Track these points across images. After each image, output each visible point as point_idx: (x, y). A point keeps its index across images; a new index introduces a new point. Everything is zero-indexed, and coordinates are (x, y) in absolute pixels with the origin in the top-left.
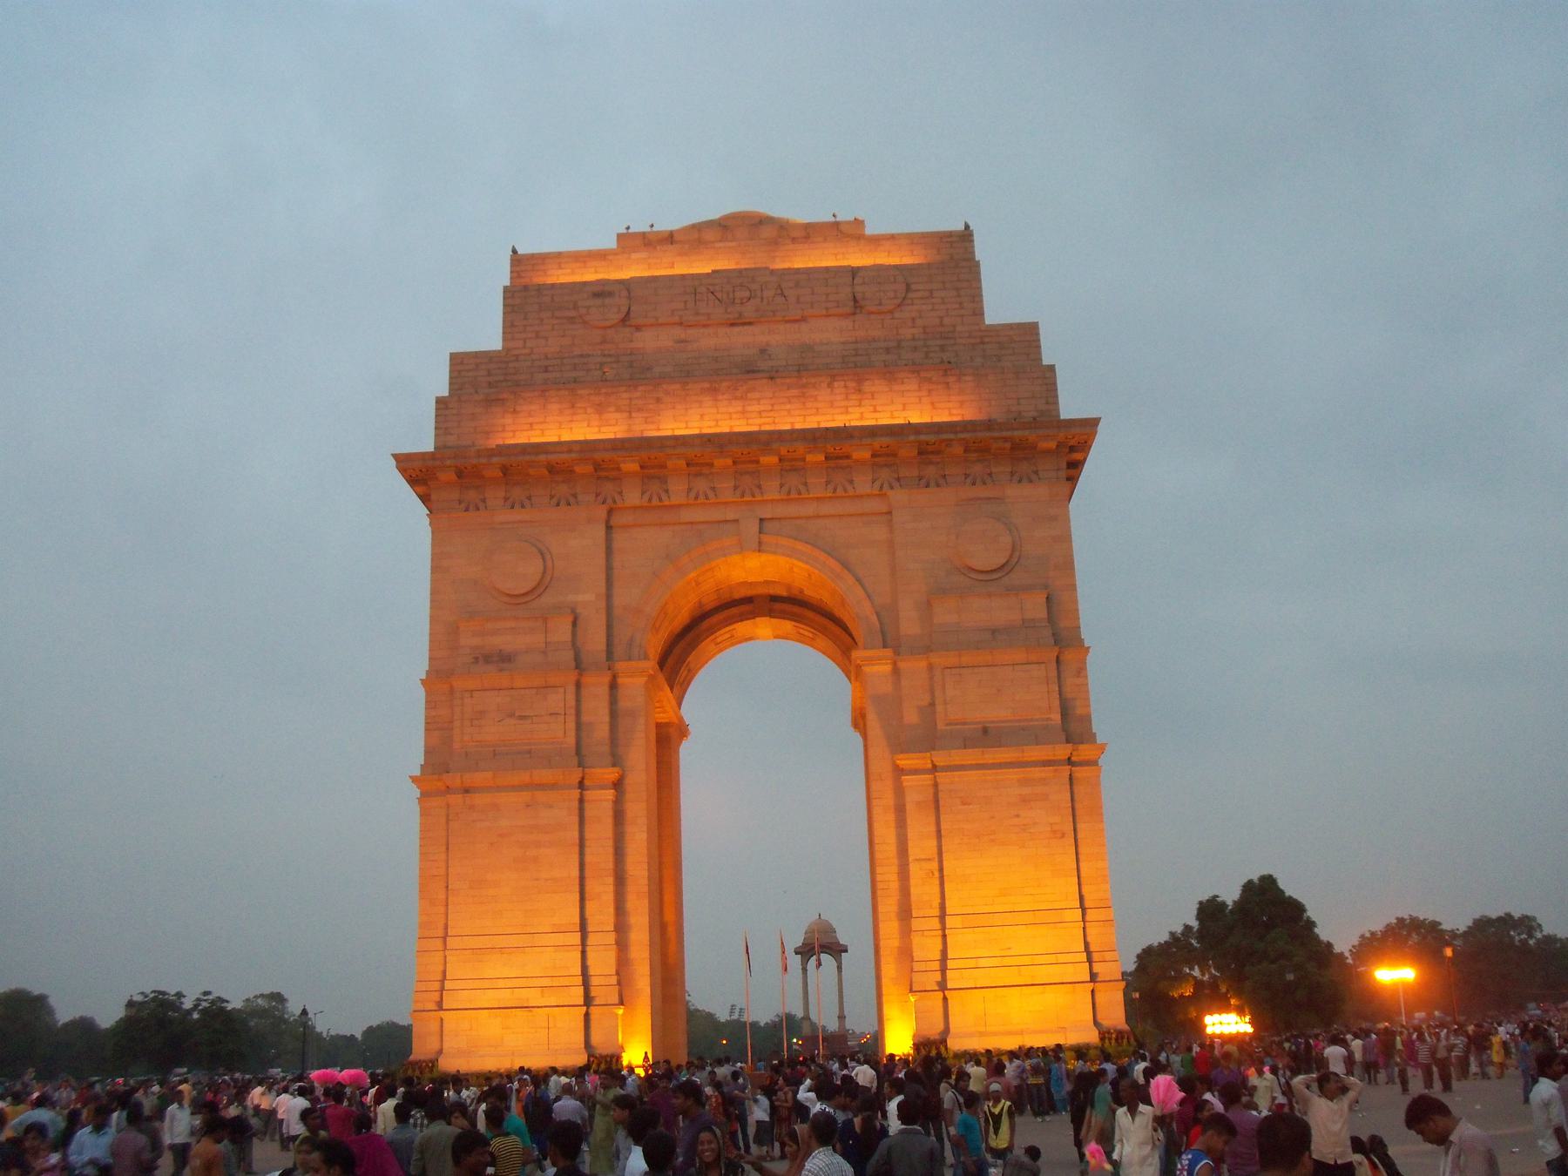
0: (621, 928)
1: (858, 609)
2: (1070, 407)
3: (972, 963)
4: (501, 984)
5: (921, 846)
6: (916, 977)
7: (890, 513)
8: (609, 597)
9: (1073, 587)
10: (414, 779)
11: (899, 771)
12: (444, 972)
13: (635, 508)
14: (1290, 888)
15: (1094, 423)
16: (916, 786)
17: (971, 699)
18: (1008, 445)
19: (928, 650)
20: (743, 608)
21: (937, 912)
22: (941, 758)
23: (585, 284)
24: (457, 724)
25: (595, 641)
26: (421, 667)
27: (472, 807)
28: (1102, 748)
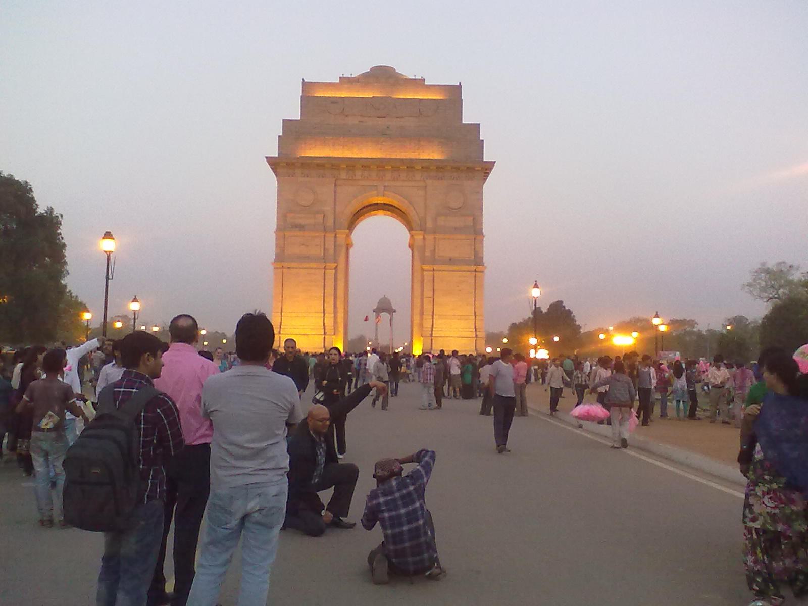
0: (335, 312)
1: (412, 215)
5: (428, 293)
7: (426, 187)
8: (335, 208)
10: (273, 264)
11: (423, 270)
12: (281, 323)
13: (344, 179)
14: (567, 305)
17: (447, 248)
18: (466, 168)
19: (435, 233)
20: (376, 206)
21: (431, 314)
25: (330, 222)
26: (274, 226)
28: (486, 268)
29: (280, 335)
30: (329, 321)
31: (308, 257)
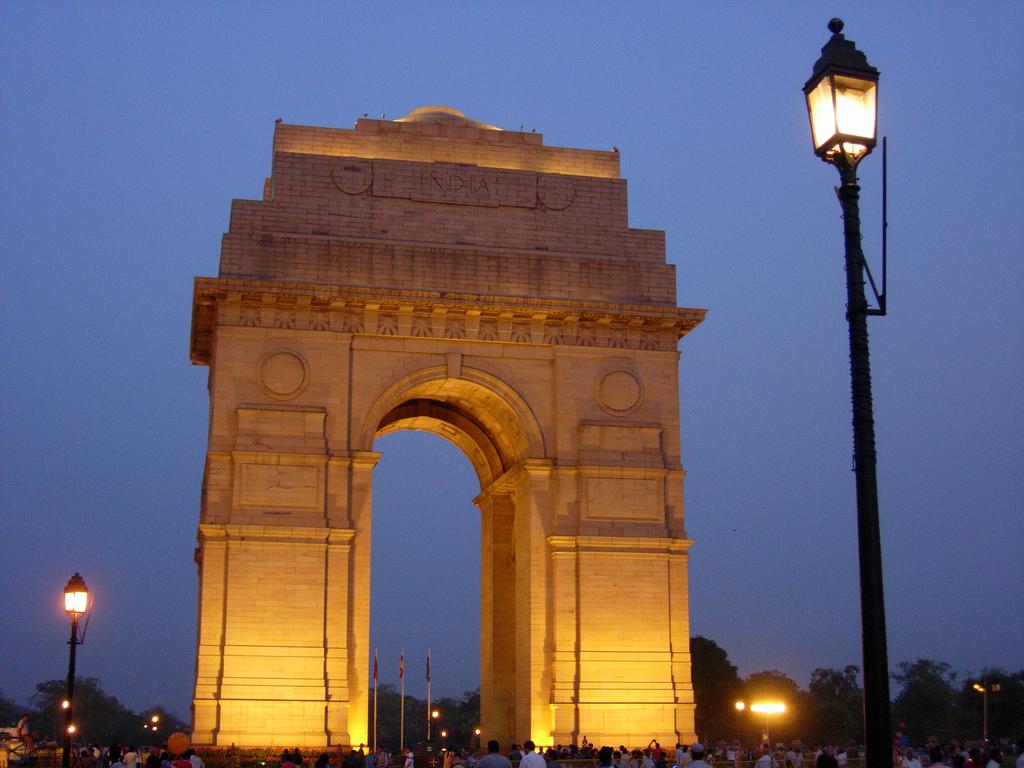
0: (351, 646)
2: (685, 300)
3: (597, 686)
4: (265, 682)
6: (556, 693)
7: (553, 362)
9: (677, 427)
11: (551, 549)
15: (705, 311)
16: (565, 559)
18: (642, 322)
22: (583, 541)
23: (339, 158)
24: (236, 487)
25: (339, 436)
27: (246, 551)
29: (221, 702)
30: (338, 669)
31: (289, 513)
